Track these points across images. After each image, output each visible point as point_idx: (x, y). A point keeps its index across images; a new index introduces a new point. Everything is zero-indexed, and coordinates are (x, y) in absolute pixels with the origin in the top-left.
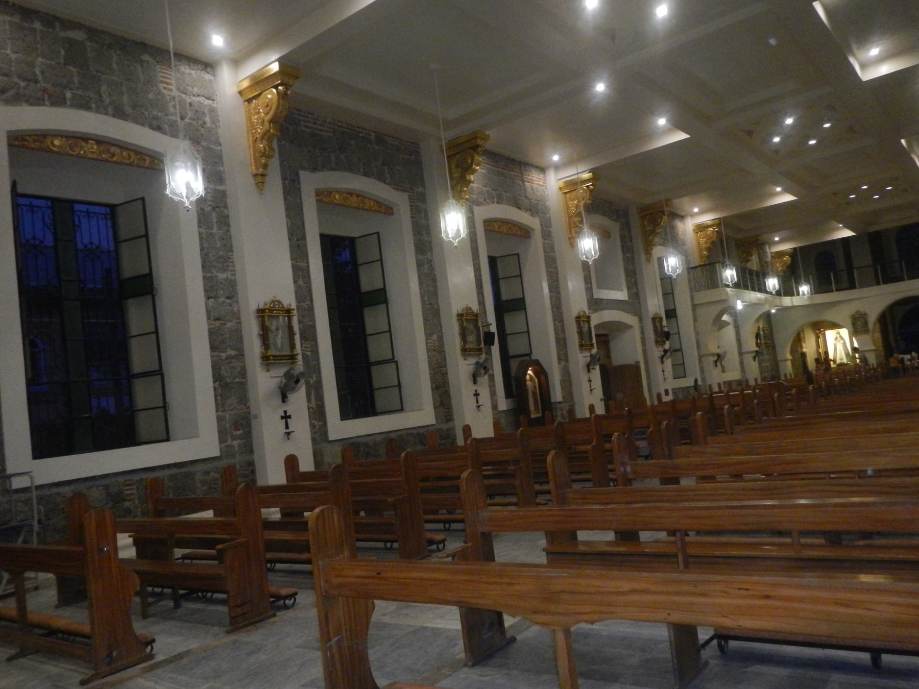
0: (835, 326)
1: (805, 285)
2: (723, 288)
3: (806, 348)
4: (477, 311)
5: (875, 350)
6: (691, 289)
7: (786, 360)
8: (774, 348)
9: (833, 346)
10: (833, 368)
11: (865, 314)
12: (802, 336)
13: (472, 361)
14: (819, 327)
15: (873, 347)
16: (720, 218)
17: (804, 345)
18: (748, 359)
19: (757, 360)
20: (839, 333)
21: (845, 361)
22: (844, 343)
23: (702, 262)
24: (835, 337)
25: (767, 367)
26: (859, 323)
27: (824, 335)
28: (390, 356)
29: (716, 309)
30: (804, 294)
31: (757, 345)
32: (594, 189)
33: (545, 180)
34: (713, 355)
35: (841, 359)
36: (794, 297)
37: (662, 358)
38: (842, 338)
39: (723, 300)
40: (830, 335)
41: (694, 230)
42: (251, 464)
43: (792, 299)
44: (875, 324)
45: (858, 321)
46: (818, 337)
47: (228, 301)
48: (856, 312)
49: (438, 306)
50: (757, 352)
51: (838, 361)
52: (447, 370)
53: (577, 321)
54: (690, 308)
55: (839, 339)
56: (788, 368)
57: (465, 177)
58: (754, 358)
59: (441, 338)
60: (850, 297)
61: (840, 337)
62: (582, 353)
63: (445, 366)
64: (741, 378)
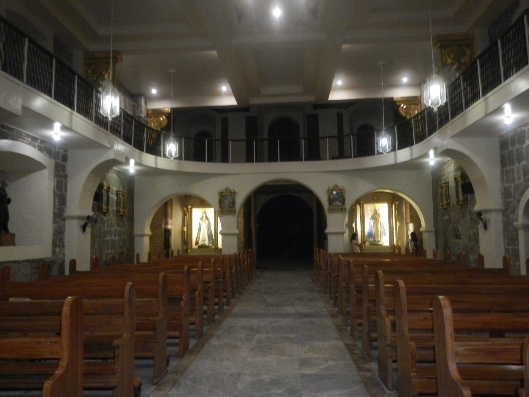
0: (203, 203)
1: (174, 142)
3: (172, 224)
5: (238, 235)
7: (143, 235)
8: (131, 218)
9: (198, 225)
10: (195, 249)
11: (234, 192)
15: (237, 231)
17: (170, 221)
19: (88, 229)
20: (205, 213)
21: (207, 243)
22: (209, 224)
24: (201, 217)
25: (113, 242)
26: (226, 201)
27: (191, 212)
30: (171, 156)
35: (203, 241)
36: (159, 158)
38: (207, 218)
40: (197, 213)
43: (156, 159)
44: (240, 209)
45: (226, 199)
46: (184, 215)
48: (225, 189)
51: (200, 243)
55: (204, 218)
58: (84, 228)
61: (206, 216)
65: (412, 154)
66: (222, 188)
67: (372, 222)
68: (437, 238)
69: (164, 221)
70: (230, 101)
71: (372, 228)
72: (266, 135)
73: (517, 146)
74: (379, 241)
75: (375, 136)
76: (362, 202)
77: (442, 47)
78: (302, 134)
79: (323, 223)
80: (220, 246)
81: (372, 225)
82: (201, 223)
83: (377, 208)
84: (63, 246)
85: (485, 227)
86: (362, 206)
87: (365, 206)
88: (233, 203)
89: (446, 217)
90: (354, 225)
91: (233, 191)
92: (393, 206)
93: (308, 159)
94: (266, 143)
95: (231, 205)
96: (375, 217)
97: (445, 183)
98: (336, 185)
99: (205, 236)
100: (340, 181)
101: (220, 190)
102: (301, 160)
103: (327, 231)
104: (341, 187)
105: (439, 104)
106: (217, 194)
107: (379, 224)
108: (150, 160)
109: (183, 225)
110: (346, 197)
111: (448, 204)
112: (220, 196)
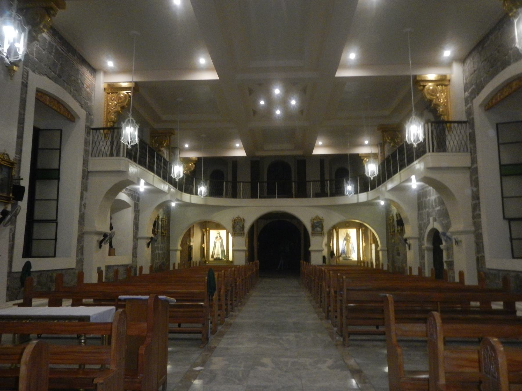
0: (218, 226)
2: (124, 158)
3: (193, 242)
5: (245, 251)
6: (86, 151)
7: (176, 250)
8: (169, 238)
10: (211, 261)
11: (244, 220)
12: (192, 232)
16: (136, 83)
17: (192, 240)
18: (142, 244)
19: (150, 246)
20: (219, 234)
21: (220, 256)
22: (222, 242)
24: (216, 237)
25: (159, 254)
26: (238, 226)
29: (113, 180)
30: (201, 194)
31: (154, 232)
34: (98, 233)
35: (218, 255)
36: (192, 196)
38: (221, 238)
40: (213, 233)
41: (105, 89)
43: (190, 197)
45: (238, 224)
46: (203, 235)
48: (237, 217)
50: (152, 238)
51: (215, 256)
55: (219, 238)
56: (176, 258)
58: (148, 245)
60: (235, 205)
61: (220, 236)
64: (131, 263)
65: (368, 197)
66: (235, 217)
67: (345, 242)
68: (388, 254)
69: (188, 239)
70: (241, 153)
71: (344, 247)
72: (265, 178)
73: (424, 199)
74: (349, 257)
75: (345, 183)
76: (337, 228)
77: (383, 132)
78: (293, 179)
79: (307, 243)
80: (231, 259)
81: (345, 245)
82: (216, 241)
83: (348, 232)
84: (136, 257)
85: (409, 249)
86: (337, 230)
87: (340, 230)
88: (243, 228)
89: (393, 241)
90: (331, 245)
91: (243, 219)
93: (297, 196)
94: (265, 185)
95: (242, 229)
96: (347, 239)
97: (392, 217)
98: (317, 215)
99: (219, 251)
100: (320, 213)
101: (233, 218)
102: (292, 197)
103: (310, 249)
104: (321, 218)
105: (374, 175)
106: (231, 221)
107: (350, 244)
108: (187, 197)
109: (202, 242)
110: (324, 225)
111: (394, 232)
112: (233, 223)
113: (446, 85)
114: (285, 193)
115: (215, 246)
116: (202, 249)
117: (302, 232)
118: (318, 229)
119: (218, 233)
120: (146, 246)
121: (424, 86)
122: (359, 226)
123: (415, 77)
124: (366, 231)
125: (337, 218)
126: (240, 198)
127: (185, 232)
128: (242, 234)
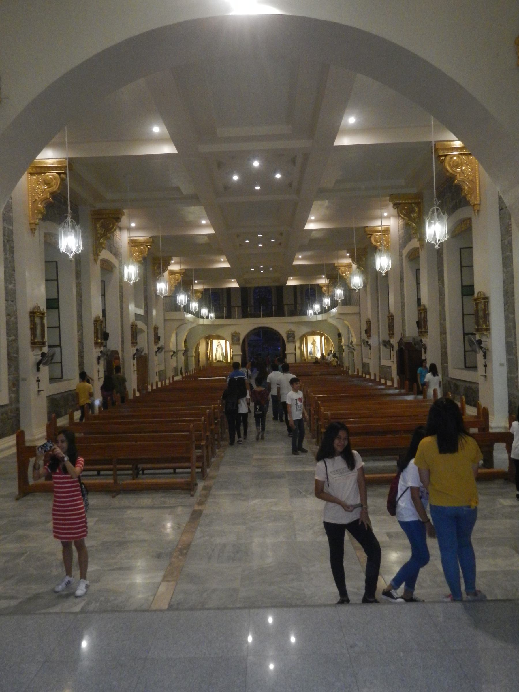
0: (219, 338)
4: (43, 310)
6: (164, 309)
7: (192, 356)
11: (239, 334)
13: (99, 350)
14: (209, 338)
18: (180, 354)
20: (219, 342)
21: (221, 359)
22: (222, 349)
23: (170, 293)
26: (235, 338)
28: (57, 343)
32: (150, 248)
33: (121, 236)
34: (171, 351)
35: (219, 358)
37: (156, 352)
38: (221, 346)
39: (182, 319)
40: (215, 342)
42: (18, 409)
43: (203, 320)
46: (207, 344)
47: (12, 303)
49: (82, 313)
50: (185, 351)
51: (218, 359)
52: (83, 354)
53: (131, 328)
54: (162, 321)
55: (219, 346)
57: (106, 235)
59: (82, 334)
61: (220, 345)
62: (132, 347)
63: (83, 352)
66: (233, 332)
67: (312, 345)
80: (229, 361)
83: (315, 339)
87: (308, 337)
88: (239, 339)
90: (302, 348)
92: (323, 337)
96: (314, 343)
100: (293, 328)
103: (286, 352)
108: (201, 321)
109: (207, 349)
113: (350, 268)
114: (269, 315)
115: (217, 352)
116: (207, 354)
117: (281, 340)
118: (291, 338)
119: (219, 342)
120: (182, 355)
121: (339, 268)
122: (321, 335)
123: (334, 264)
124: (326, 339)
125: (304, 330)
126: (235, 318)
127: (197, 344)
128: (238, 344)
